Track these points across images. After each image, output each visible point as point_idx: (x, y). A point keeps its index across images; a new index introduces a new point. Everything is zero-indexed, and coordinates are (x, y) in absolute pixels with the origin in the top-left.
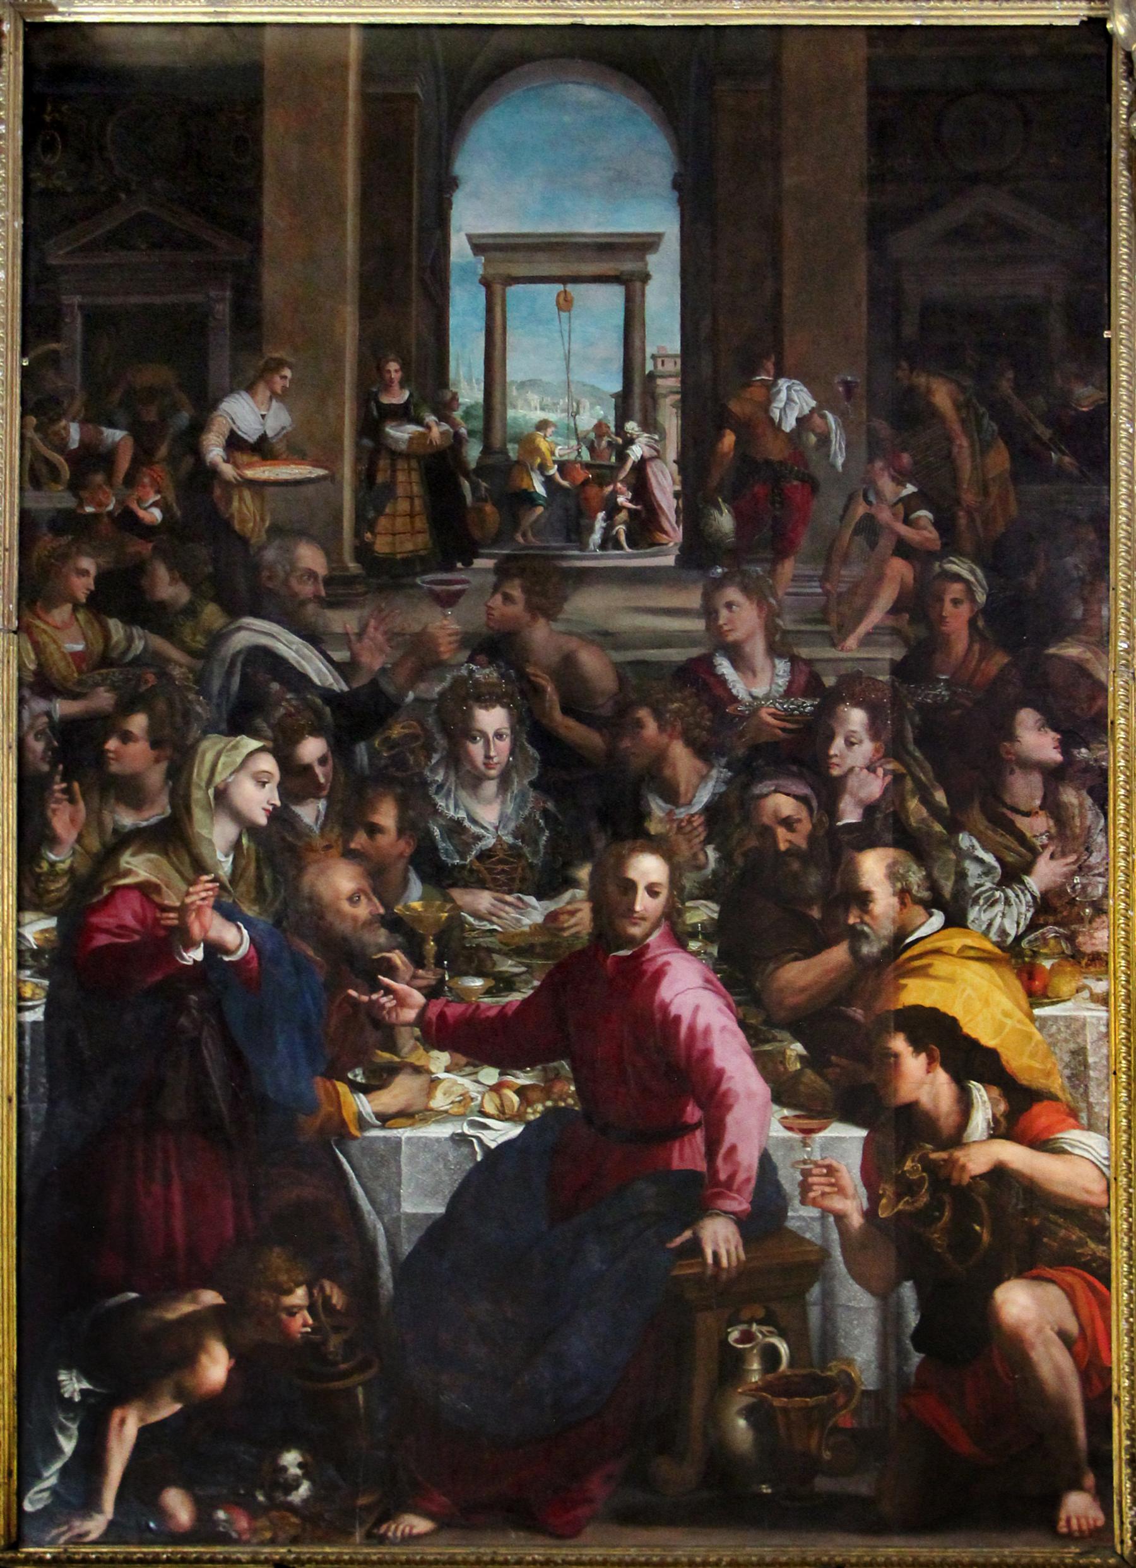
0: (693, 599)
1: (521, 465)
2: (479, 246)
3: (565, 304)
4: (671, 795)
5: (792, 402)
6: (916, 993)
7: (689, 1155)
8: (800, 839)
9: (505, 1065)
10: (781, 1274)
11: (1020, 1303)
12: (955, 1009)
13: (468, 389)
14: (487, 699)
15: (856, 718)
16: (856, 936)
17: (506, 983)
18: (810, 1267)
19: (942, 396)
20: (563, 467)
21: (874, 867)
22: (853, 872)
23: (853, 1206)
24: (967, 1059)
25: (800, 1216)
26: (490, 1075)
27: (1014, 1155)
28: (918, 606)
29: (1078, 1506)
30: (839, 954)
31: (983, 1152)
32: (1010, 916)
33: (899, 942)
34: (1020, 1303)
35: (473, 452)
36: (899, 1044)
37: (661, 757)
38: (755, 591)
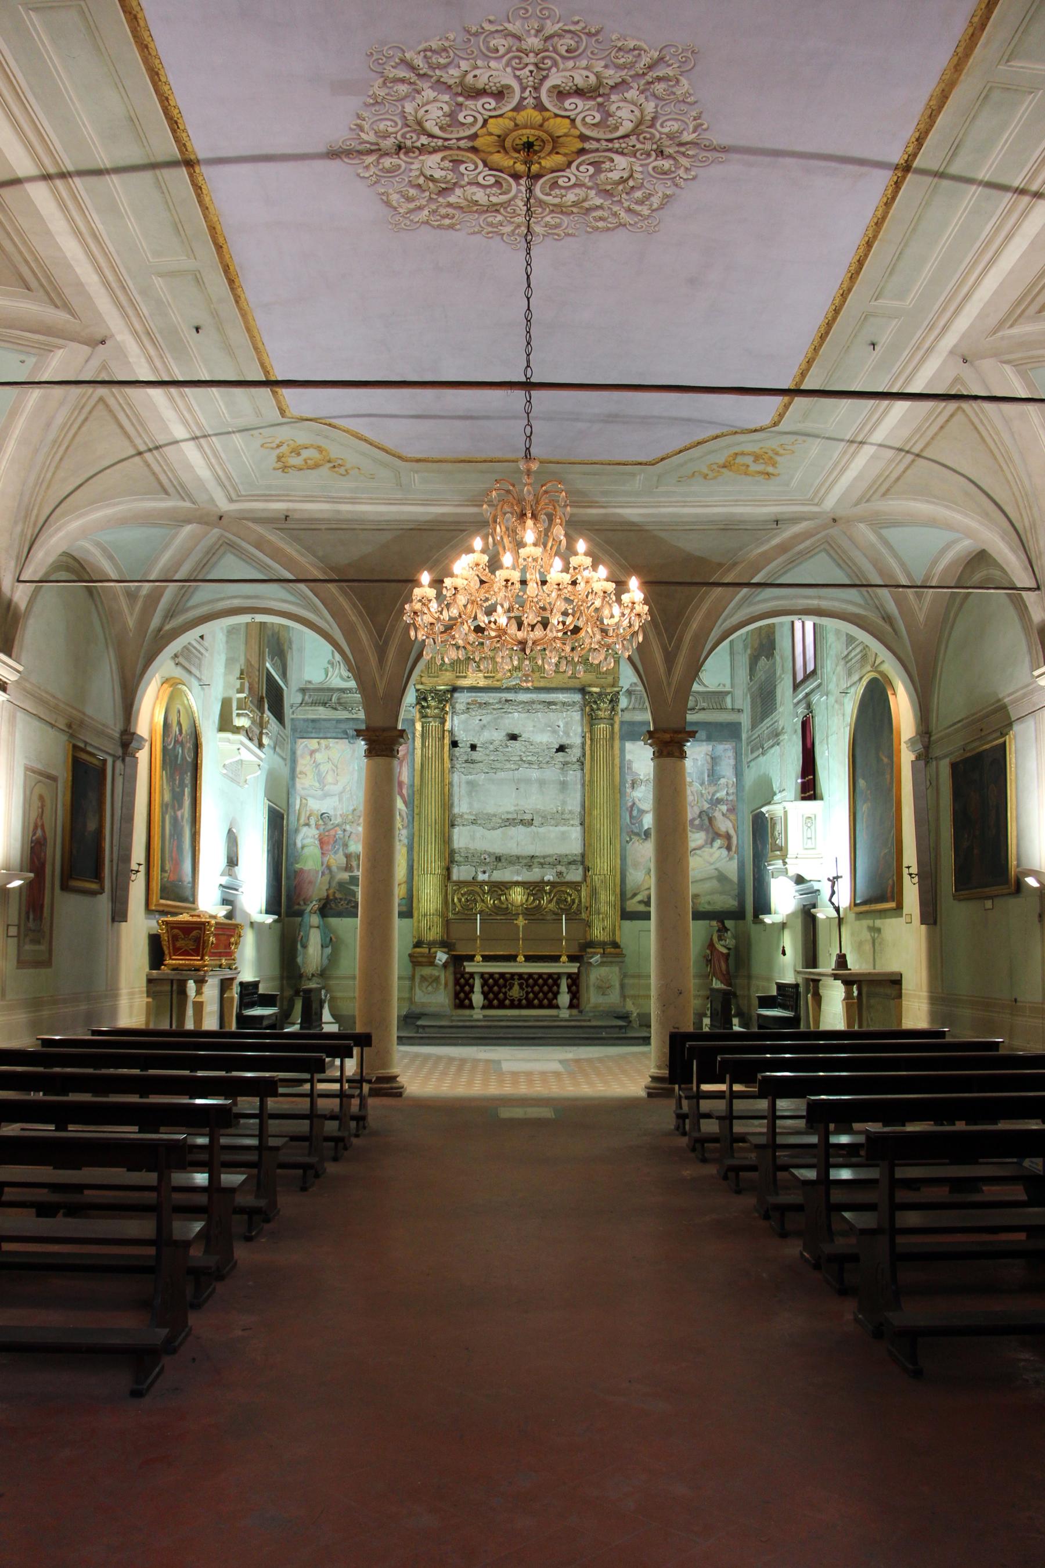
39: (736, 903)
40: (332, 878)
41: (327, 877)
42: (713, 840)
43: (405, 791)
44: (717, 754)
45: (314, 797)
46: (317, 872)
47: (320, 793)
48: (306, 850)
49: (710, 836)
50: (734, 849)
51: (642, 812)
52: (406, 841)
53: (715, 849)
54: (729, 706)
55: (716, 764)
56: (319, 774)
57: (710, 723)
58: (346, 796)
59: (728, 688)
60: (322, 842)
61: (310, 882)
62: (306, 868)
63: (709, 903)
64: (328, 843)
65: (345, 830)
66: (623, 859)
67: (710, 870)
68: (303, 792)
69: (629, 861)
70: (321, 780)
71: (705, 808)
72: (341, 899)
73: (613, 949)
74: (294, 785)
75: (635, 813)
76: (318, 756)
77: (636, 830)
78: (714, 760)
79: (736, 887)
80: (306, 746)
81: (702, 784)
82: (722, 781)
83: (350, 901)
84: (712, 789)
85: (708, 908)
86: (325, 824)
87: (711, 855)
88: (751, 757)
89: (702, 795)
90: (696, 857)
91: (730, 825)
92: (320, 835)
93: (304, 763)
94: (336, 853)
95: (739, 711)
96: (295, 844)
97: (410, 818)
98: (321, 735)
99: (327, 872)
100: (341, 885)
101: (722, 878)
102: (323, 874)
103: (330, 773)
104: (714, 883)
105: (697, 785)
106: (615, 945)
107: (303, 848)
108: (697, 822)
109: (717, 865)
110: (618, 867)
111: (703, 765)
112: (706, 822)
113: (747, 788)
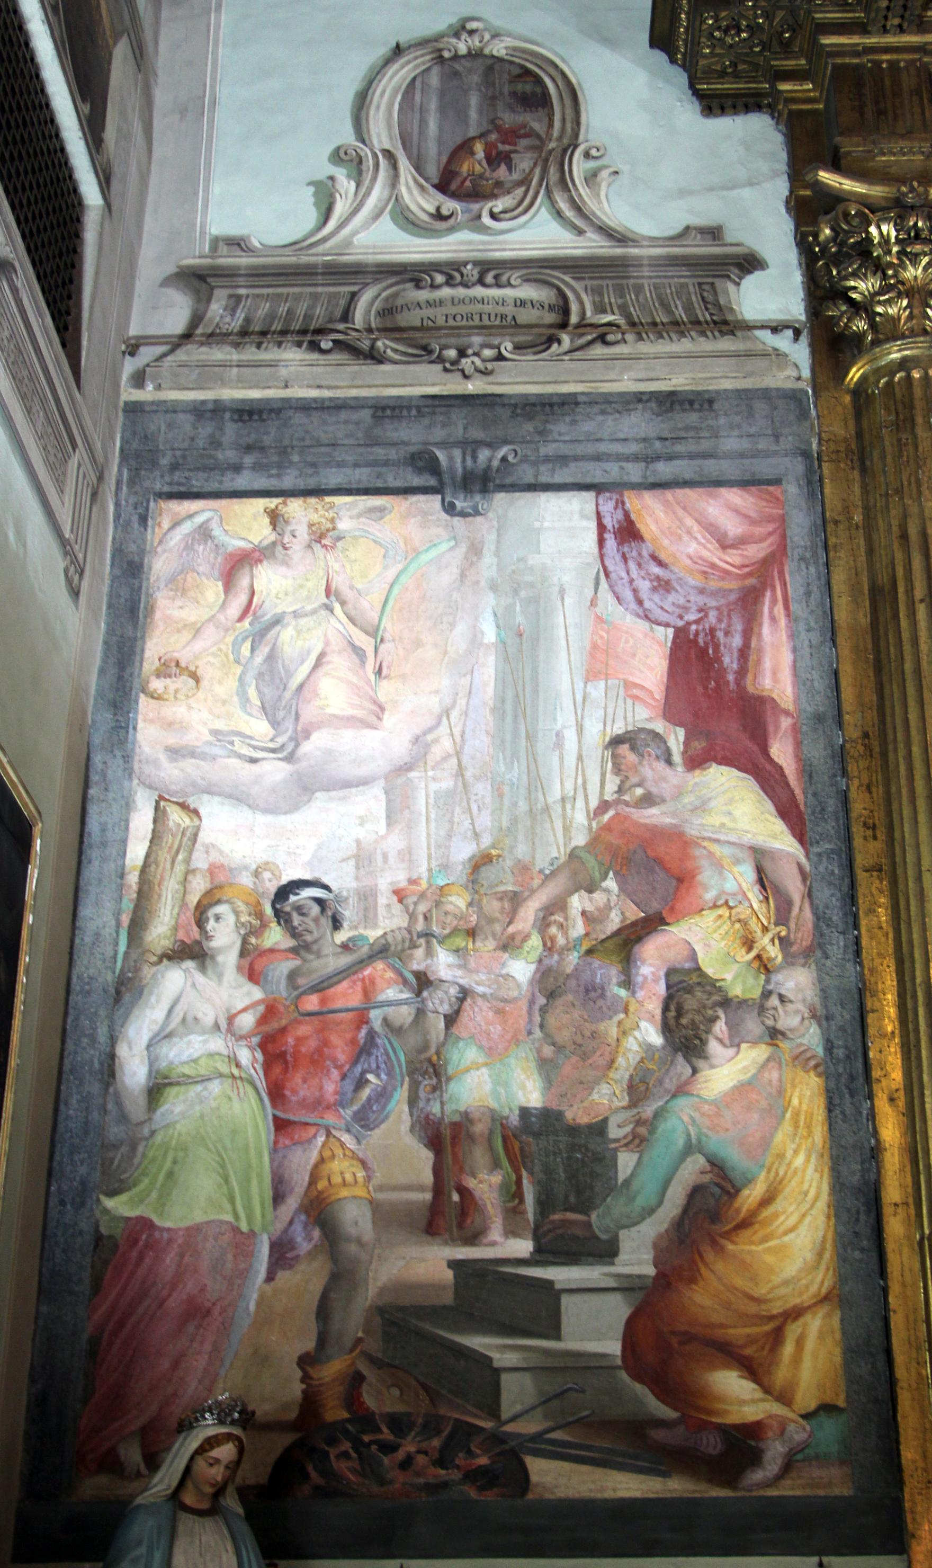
40: (342, 1277)
41: (307, 1279)
43: (781, 751)
45: (237, 796)
46: (242, 1242)
47: (274, 771)
48: (177, 1107)
52: (812, 1038)
56: (273, 670)
58: (428, 786)
60: (279, 1053)
61: (197, 1312)
62: (175, 1217)
64: (318, 1060)
65: (423, 982)
68: (171, 773)
70: (284, 702)
72: (398, 1423)
74: (122, 729)
76: (269, 581)
80: (204, 533)
83: (463, 1435)
86: (302, 947)
92: (270, 1011)
93: (186, 619)
94: (365, 1120)
96: (109, 1068)
97: (829, 896)
98: (289, 481)
99: (305, 1240)
100: (404, 1324)
102: (282, 1253)
103: (340, 663)
107: (157, 1089)
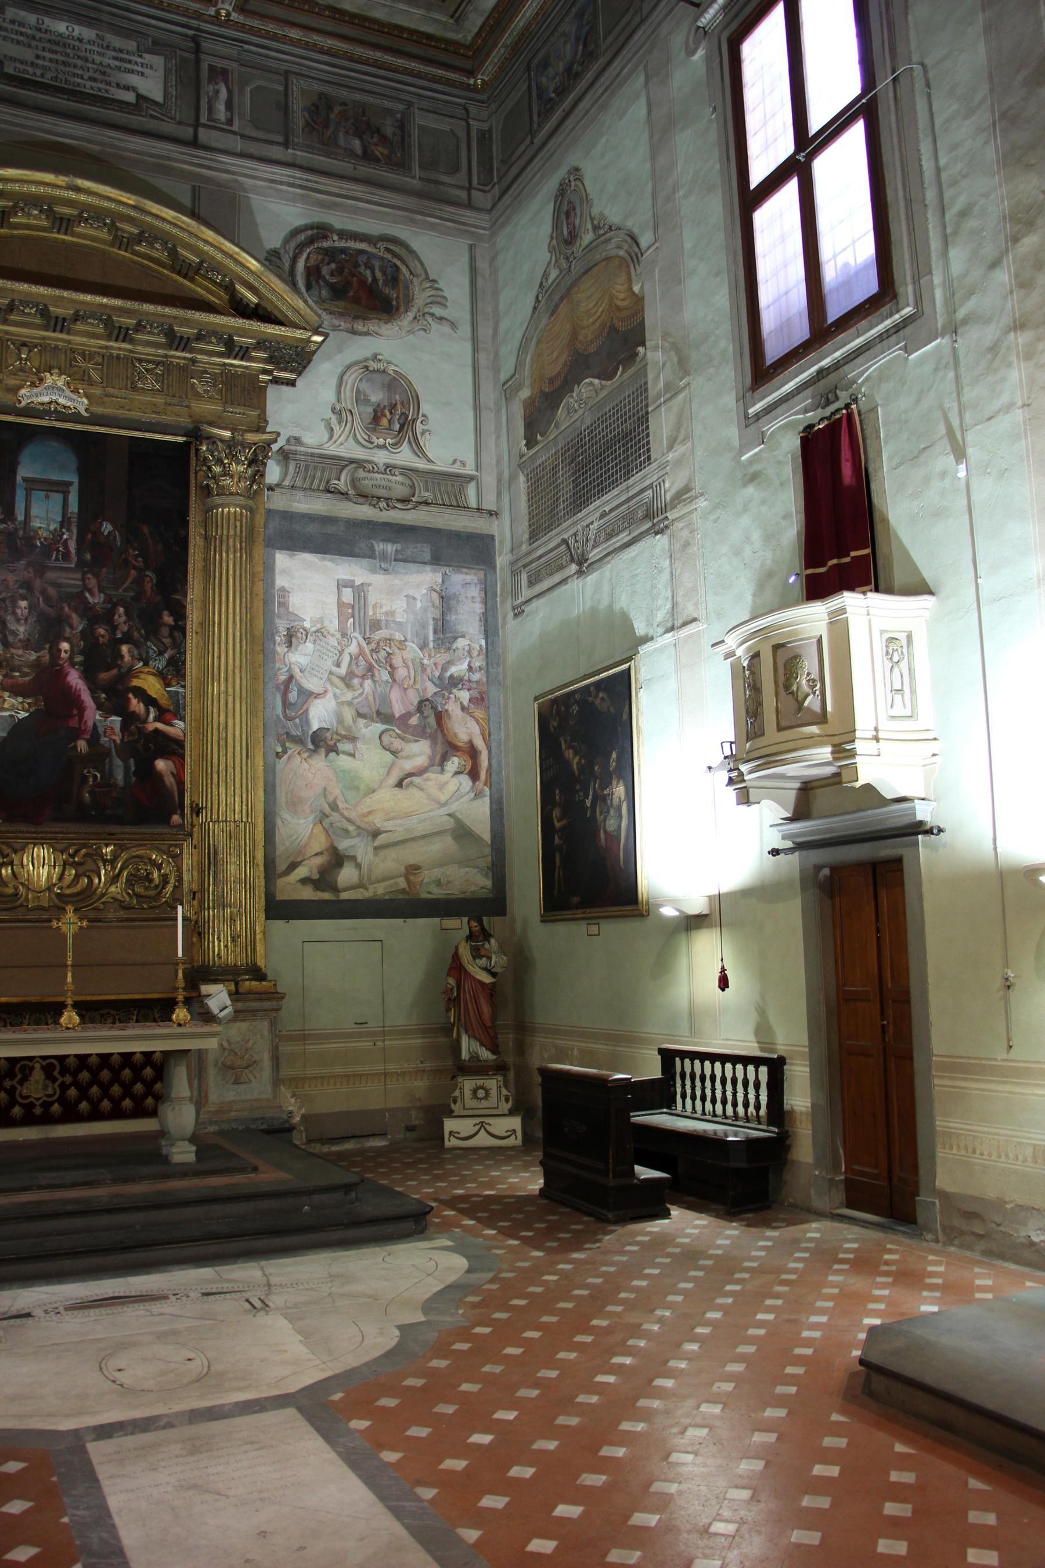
0: (79, 576)
1: (33, 538)
2: (24, 479)
3: (47, 497)
4: (72, 627)
5: (107, 528)
6: (135, 682)
7: (73, 723)
8: (106, 640)
9: (25, 697)
10: (98, 755)
11: (161, 764)
12: (145, 687)
13: (21, 517)
14: (24, 598)
15: (121, 610)
16: (120, 667)
17: (25, 675)
18: (107, 753)
19: (146, 530)
20: (46, 539)
21: (125, 649)
22: (119, 650)
23: (117, 739)
24: (149, 701)
25: (104, 740)
26: (20, 699)
27: (160, 726)
28: (139, 582)
29: (176, 818)
30: (115, 671)
31: (152, 725)
32: (161, 663)
33: (130, 669)
34: (161, 764)
35: (21, 533)
36: (131, 696)
37: (69, 617)
38: (96, 576)
39: (488, 883)
42: (444, 758)
44: (452, 590)
49: (439, 749)
50: (483, 775)
51: (308, 695)
53: (448, 775)
54: (473, 502)
55: (449, 609)
57: (438, 531)
59: (469, 470)
63: (439, 883)
66: (270, 790)
67: (440, 818)
69: (281, 796)
71: (429, 695)
73: (253, 985)
75: (293, 696)
77: (294, 732)
78: (446, 602)
79: (488, 850)
81: (423, 647)
82: (461, 643)
84: (442, 658)
85: (437, 893)
87: (442, 787)
88: (526, 593)
89: (424, 668)
90: (413, 791)
91: (476, 730)
95: (490, 513)
101: (462, 832)
104: (448, 842)
105: (412, 649)
106: (259, 975)
108: (414, 721)
109: (454, 807)
110: (260, 807)
111: (425, 610)
112: (432, 720)
113: (511, 658)
